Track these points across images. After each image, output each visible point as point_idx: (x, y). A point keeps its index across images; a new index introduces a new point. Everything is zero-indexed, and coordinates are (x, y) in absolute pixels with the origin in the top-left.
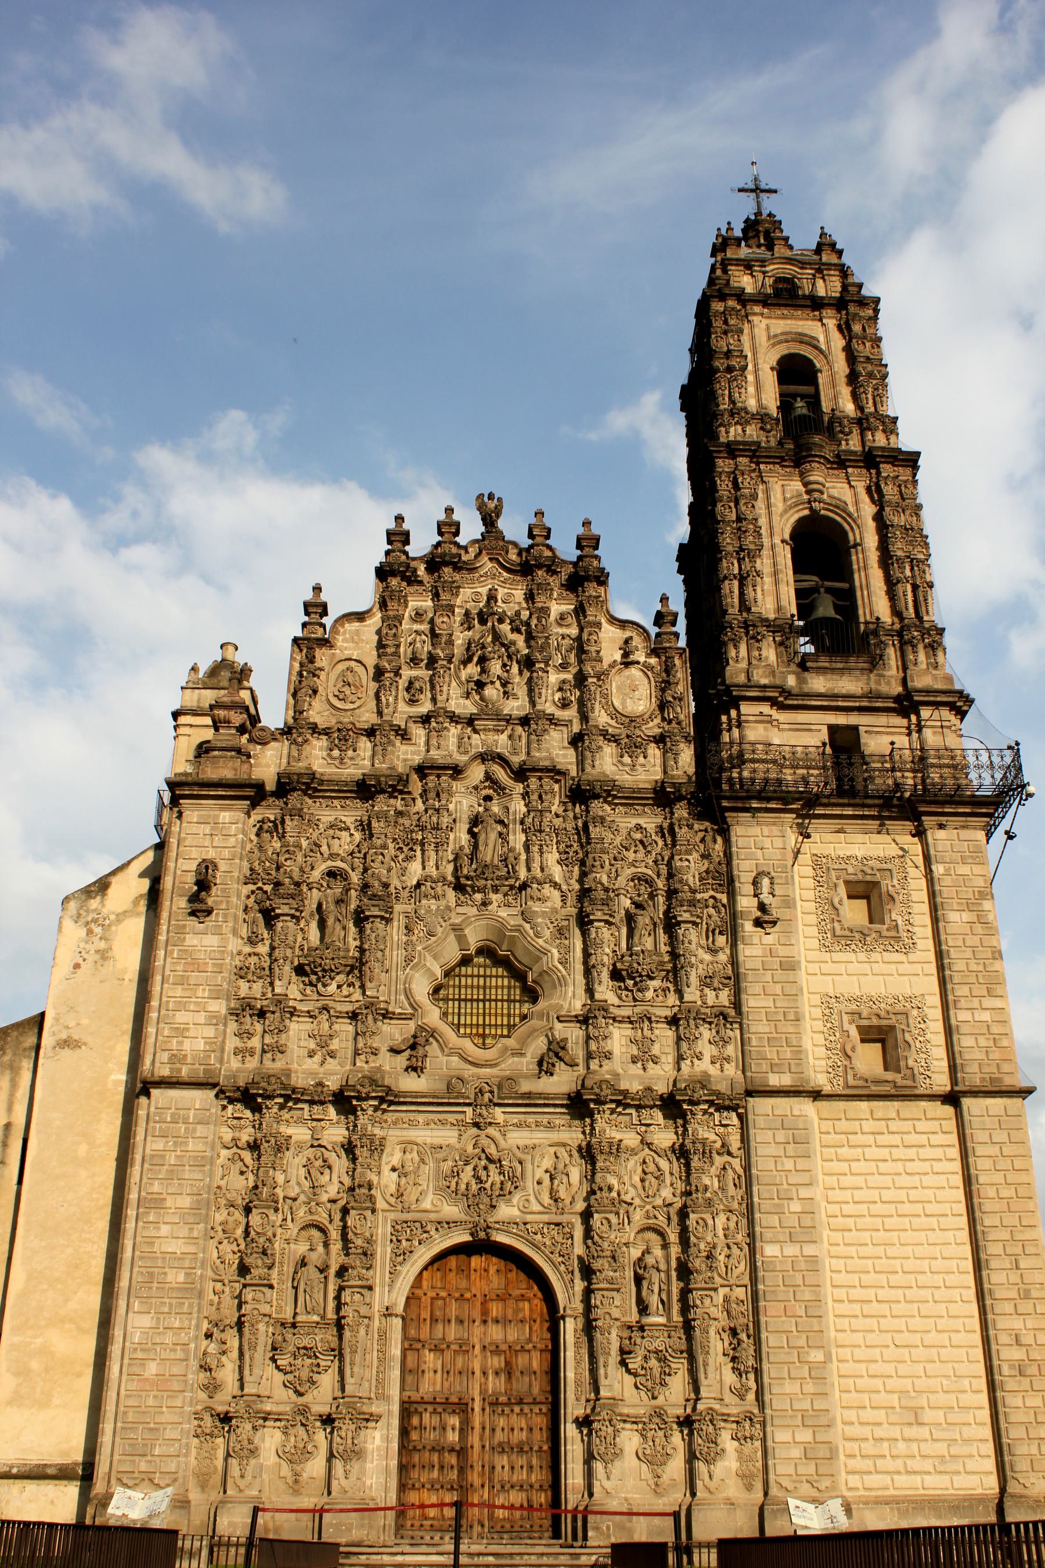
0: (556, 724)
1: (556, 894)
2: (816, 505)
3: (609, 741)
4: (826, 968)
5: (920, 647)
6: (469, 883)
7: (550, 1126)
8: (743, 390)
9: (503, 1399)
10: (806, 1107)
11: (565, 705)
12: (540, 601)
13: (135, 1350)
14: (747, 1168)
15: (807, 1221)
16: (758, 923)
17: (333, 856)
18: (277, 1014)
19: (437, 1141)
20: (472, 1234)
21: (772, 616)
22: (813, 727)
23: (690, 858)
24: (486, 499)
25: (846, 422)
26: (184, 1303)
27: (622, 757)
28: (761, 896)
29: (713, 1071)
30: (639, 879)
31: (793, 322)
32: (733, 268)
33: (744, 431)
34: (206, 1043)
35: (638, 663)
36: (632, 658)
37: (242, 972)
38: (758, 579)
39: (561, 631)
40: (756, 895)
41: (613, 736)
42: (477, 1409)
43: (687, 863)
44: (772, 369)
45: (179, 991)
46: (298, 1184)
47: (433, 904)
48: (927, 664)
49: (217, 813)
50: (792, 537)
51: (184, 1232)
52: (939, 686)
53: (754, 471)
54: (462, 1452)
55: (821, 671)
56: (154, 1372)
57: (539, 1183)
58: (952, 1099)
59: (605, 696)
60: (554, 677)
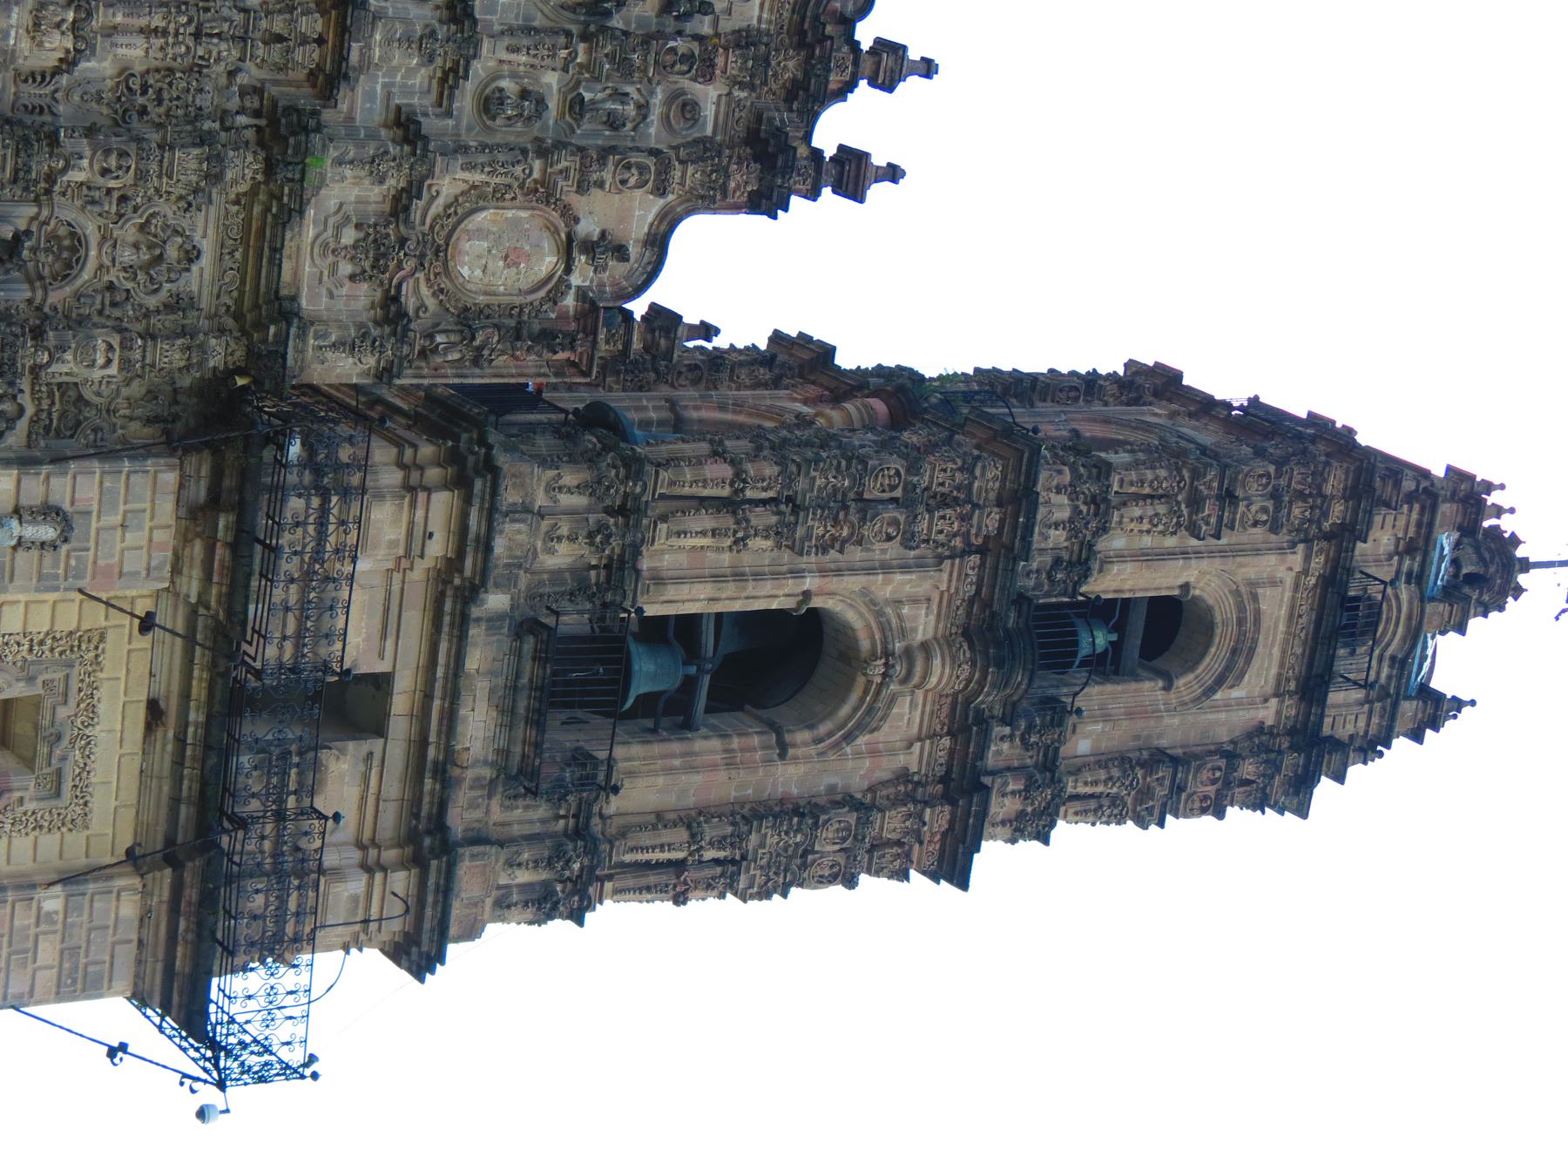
0: (443, 80)
1: (50, 60)
2: (878, 668)
3: (396, 199)
5: (544, 875)
8: (1146, 526)
11: (490, 104)
12: (729, 62)
21: (645, 564)
22: (390, 643)
23: (113, 370)
25: (1047, 739)
27: (358, 226)
28: (15, 523)
30: (73, 250)
31: (1280, 637)
32: (1415, 516)
33: (1056, 525)
35: (568, 270)
36: (581, 260)
38: (728, 542)
39: (658, 99)
40: (17, 511)
41: (407, 209)
43: (101, 361)
44: (1185, 587)
48: (507, 887)
50: (814, 612)
52: (457, 910)
53: (966, 537)
59: (499, 196)
60: (551, 80)
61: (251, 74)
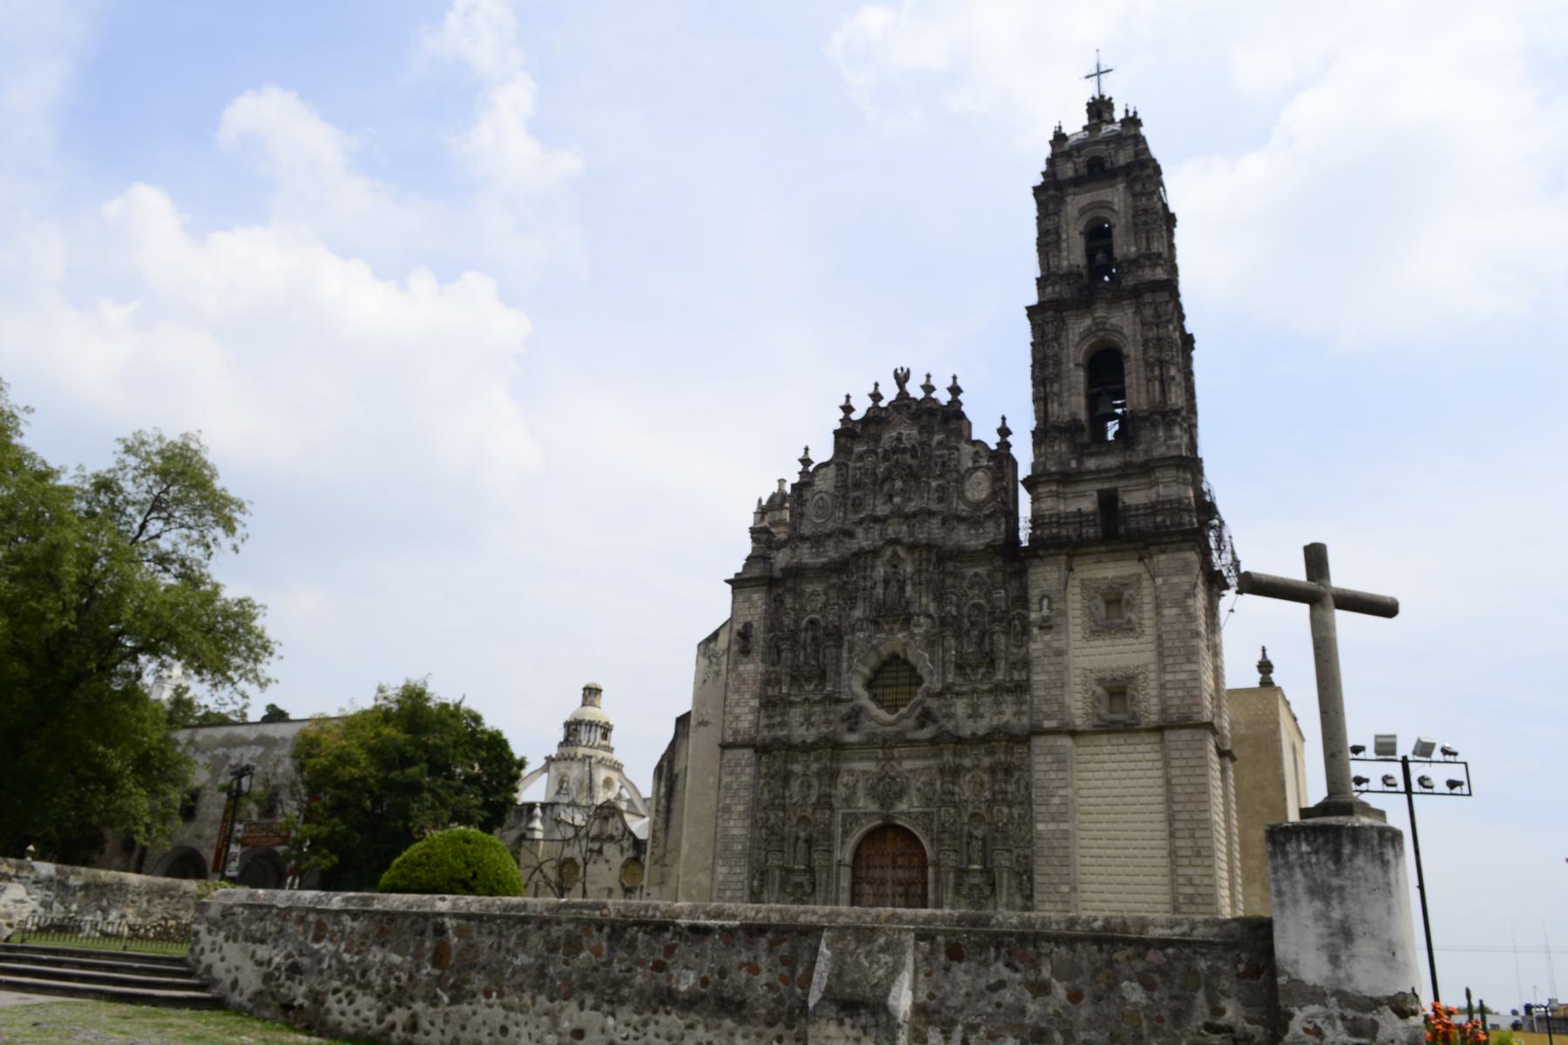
4: (1085, 652)
7: (926, 757)
10: (1067, 742)
11: (941, 500)
14: (1031, 776)
15: (1063, 809)
16: (1041, 628)
17: (813, 611)
29: (1014, 721)
37: (767, 682)
39: (938, 453)
45: (736, 697)
47: (861, 635)
51: (740, 824)
55: (1093, 455)
57: (919, 790)
58: (1159, 729)
60: (934, 484)
61: (931, 569)
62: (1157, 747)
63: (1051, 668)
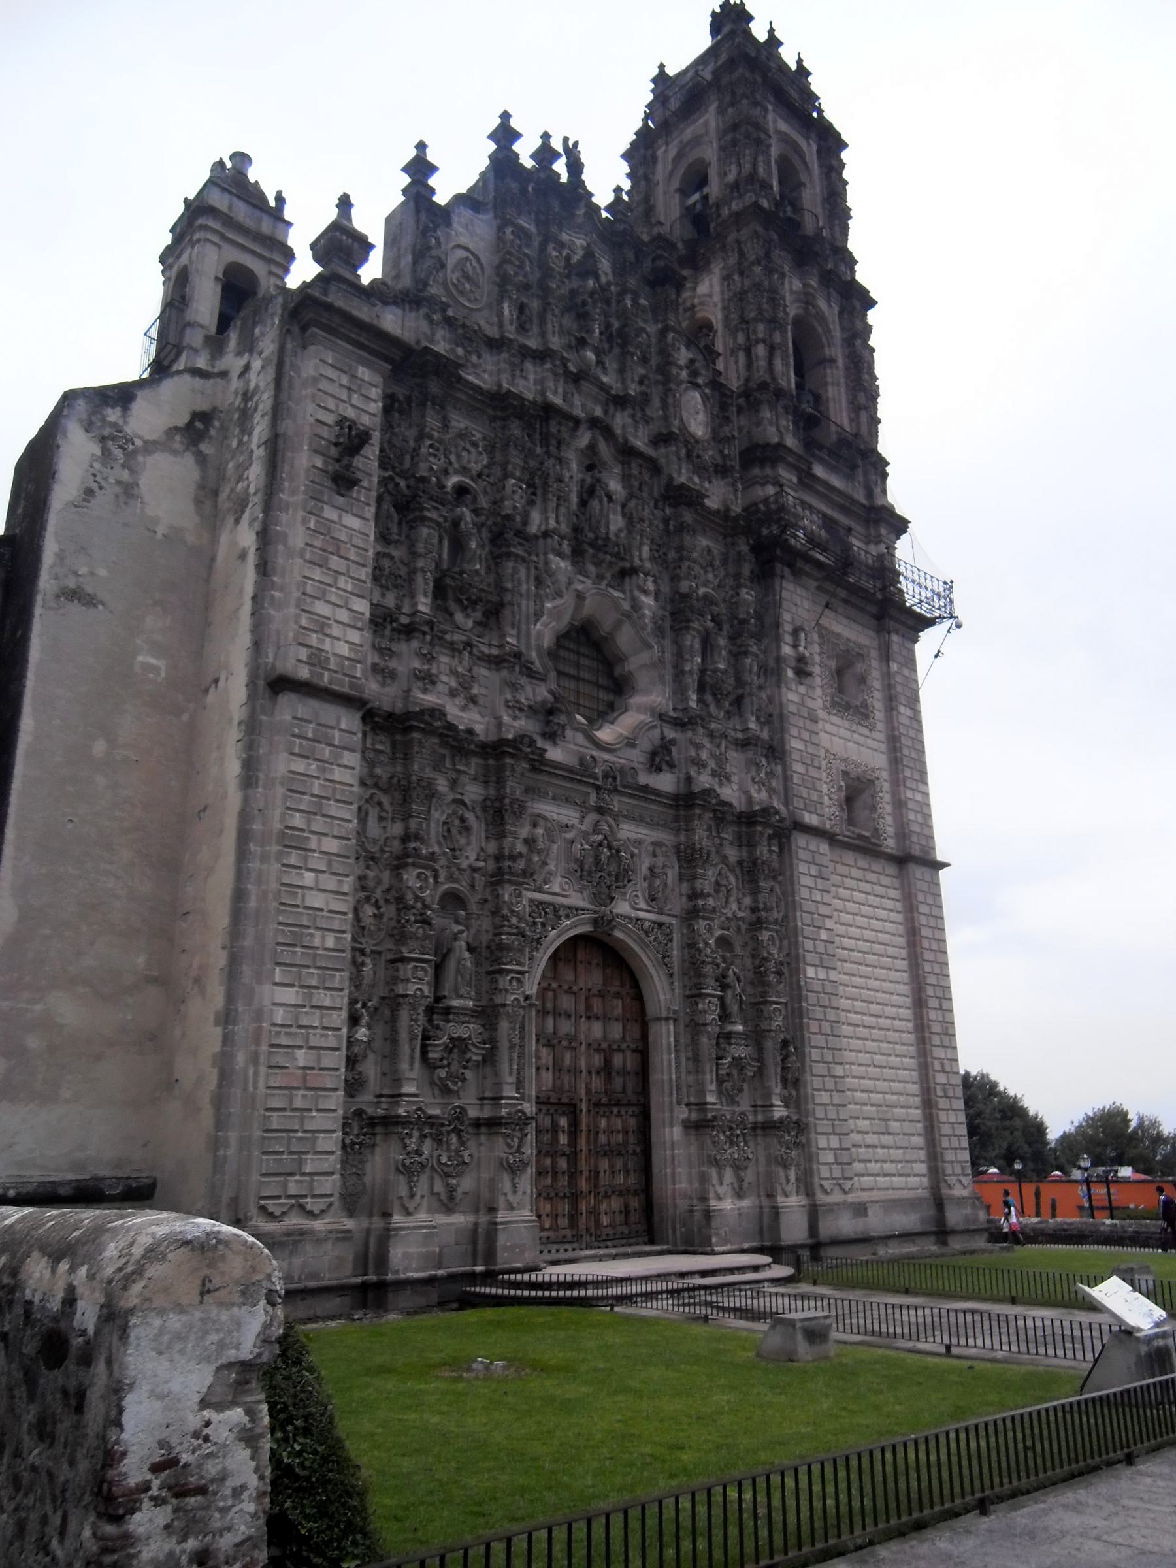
6: (591, 551)
9: (604, 1100)
10: (824, 847)
13: (278, 1033)
18: (428, 638)
19: (565, 820)
20: (595, 922)
24: (570, 144)
26: (334, 976)
34: (350, 649)
42: (584, 1111)
45: (317, 574)
46: (439, 843)
49: (354, 364)
51: (330, 883)
54: (573, 1157)
56: (301, 1064)
62: (896, 883)
63: (806, 736)
